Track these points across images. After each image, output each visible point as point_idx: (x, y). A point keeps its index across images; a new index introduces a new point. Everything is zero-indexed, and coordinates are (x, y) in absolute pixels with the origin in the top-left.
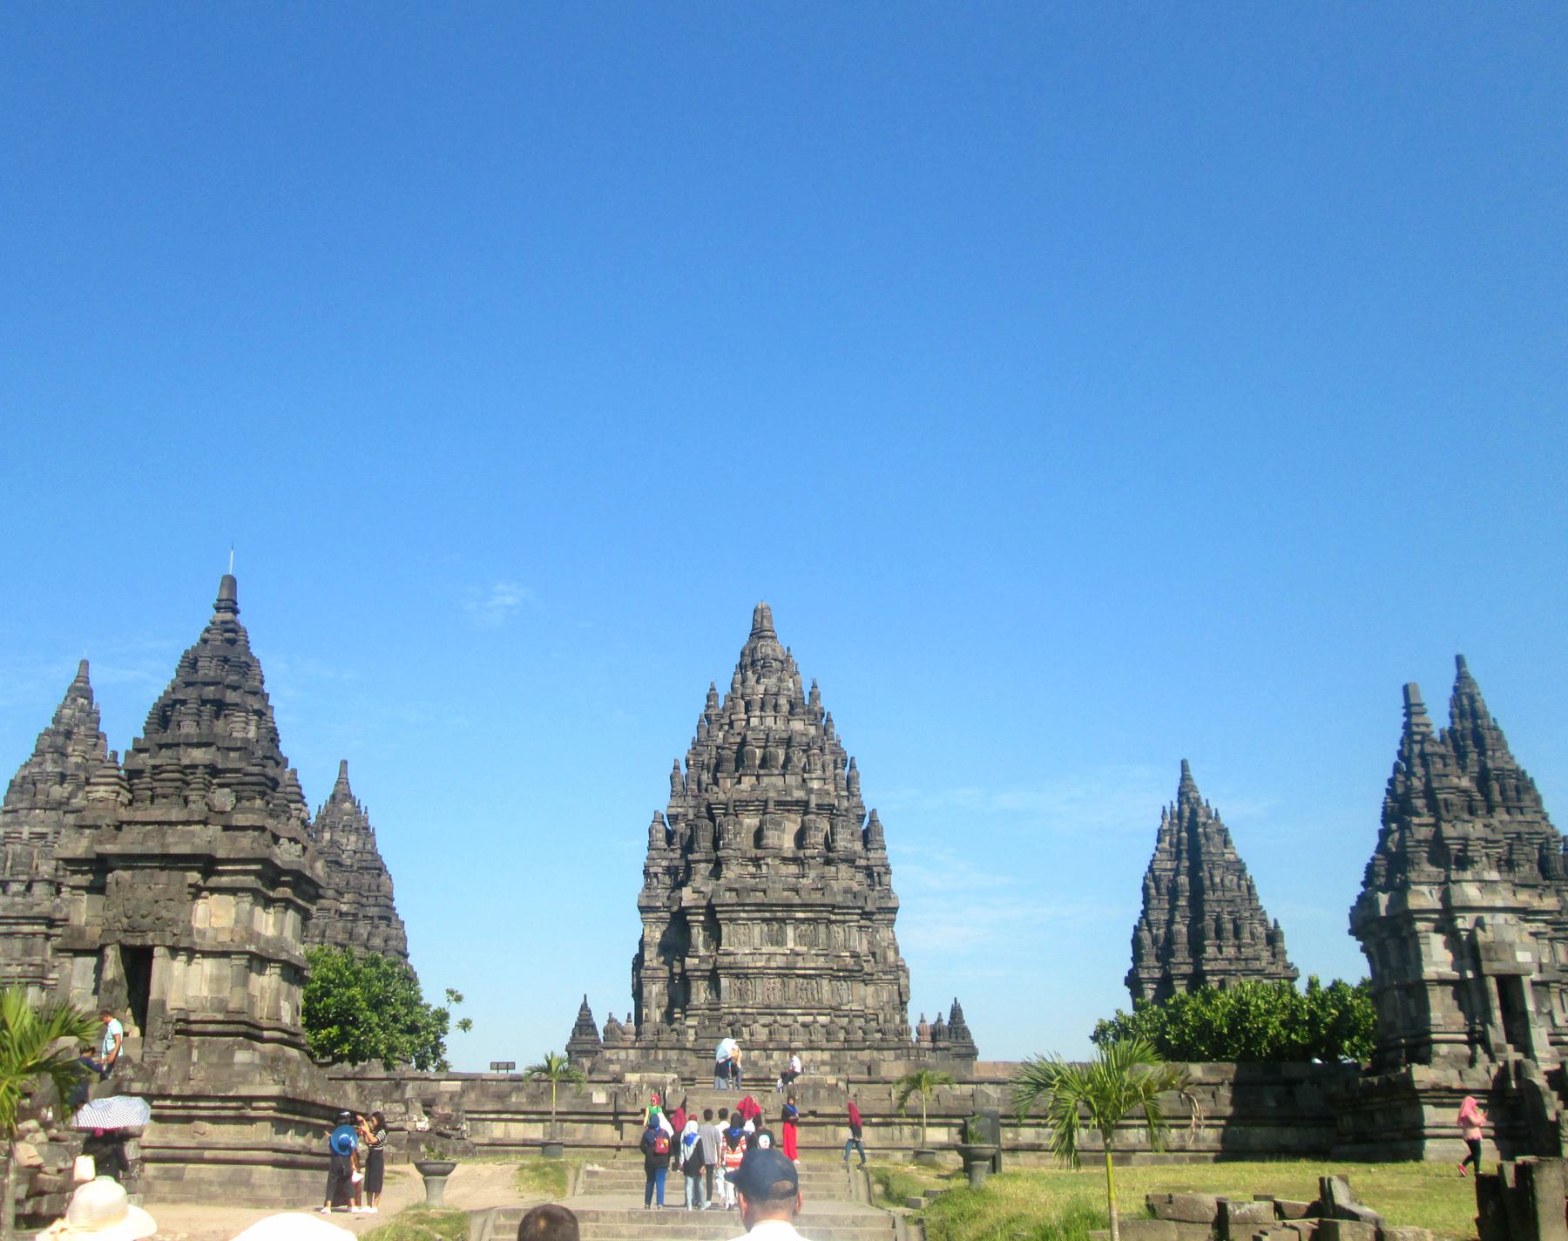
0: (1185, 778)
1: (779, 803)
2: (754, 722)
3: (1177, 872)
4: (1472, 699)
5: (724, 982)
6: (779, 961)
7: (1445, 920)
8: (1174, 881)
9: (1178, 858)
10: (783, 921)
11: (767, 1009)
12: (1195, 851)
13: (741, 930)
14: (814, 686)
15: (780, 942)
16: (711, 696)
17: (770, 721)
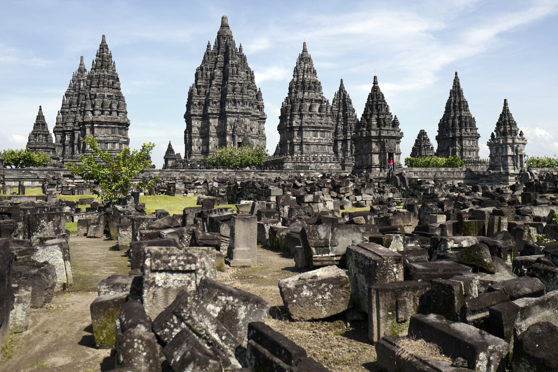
0: (342, 84)
1: (315, 100)
2: (305, 76)
3: (339, 111)
4: (459, 83)
5: (304, 146)
6: (317, 141)
7: (512, 145)
8: (338, 115)
9: (339, 107)
10: (318, 131)
11: (314, 153)
12: (345, 106)
13: (307, 133)
14: (241, 46)
15: (316, 136)
16: (209, 46)
17: (309, 76)
